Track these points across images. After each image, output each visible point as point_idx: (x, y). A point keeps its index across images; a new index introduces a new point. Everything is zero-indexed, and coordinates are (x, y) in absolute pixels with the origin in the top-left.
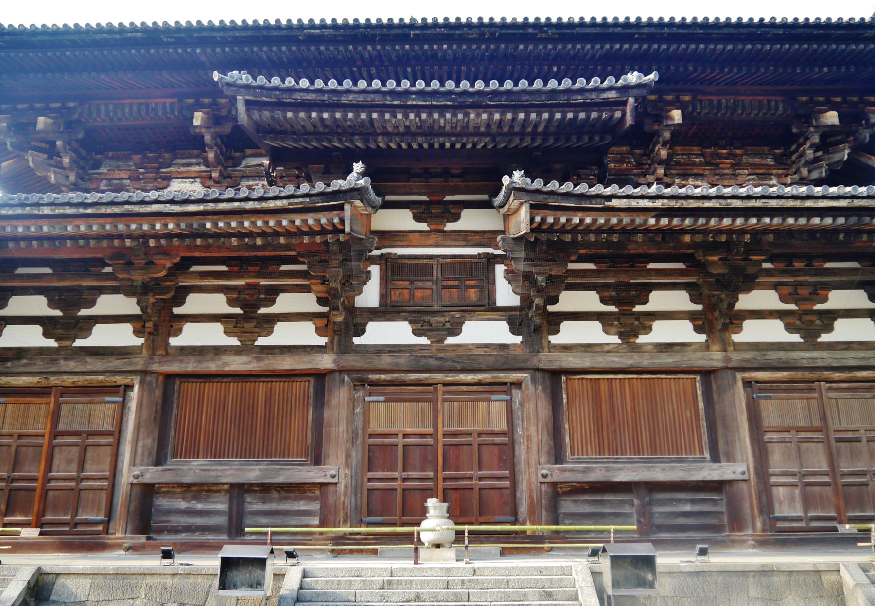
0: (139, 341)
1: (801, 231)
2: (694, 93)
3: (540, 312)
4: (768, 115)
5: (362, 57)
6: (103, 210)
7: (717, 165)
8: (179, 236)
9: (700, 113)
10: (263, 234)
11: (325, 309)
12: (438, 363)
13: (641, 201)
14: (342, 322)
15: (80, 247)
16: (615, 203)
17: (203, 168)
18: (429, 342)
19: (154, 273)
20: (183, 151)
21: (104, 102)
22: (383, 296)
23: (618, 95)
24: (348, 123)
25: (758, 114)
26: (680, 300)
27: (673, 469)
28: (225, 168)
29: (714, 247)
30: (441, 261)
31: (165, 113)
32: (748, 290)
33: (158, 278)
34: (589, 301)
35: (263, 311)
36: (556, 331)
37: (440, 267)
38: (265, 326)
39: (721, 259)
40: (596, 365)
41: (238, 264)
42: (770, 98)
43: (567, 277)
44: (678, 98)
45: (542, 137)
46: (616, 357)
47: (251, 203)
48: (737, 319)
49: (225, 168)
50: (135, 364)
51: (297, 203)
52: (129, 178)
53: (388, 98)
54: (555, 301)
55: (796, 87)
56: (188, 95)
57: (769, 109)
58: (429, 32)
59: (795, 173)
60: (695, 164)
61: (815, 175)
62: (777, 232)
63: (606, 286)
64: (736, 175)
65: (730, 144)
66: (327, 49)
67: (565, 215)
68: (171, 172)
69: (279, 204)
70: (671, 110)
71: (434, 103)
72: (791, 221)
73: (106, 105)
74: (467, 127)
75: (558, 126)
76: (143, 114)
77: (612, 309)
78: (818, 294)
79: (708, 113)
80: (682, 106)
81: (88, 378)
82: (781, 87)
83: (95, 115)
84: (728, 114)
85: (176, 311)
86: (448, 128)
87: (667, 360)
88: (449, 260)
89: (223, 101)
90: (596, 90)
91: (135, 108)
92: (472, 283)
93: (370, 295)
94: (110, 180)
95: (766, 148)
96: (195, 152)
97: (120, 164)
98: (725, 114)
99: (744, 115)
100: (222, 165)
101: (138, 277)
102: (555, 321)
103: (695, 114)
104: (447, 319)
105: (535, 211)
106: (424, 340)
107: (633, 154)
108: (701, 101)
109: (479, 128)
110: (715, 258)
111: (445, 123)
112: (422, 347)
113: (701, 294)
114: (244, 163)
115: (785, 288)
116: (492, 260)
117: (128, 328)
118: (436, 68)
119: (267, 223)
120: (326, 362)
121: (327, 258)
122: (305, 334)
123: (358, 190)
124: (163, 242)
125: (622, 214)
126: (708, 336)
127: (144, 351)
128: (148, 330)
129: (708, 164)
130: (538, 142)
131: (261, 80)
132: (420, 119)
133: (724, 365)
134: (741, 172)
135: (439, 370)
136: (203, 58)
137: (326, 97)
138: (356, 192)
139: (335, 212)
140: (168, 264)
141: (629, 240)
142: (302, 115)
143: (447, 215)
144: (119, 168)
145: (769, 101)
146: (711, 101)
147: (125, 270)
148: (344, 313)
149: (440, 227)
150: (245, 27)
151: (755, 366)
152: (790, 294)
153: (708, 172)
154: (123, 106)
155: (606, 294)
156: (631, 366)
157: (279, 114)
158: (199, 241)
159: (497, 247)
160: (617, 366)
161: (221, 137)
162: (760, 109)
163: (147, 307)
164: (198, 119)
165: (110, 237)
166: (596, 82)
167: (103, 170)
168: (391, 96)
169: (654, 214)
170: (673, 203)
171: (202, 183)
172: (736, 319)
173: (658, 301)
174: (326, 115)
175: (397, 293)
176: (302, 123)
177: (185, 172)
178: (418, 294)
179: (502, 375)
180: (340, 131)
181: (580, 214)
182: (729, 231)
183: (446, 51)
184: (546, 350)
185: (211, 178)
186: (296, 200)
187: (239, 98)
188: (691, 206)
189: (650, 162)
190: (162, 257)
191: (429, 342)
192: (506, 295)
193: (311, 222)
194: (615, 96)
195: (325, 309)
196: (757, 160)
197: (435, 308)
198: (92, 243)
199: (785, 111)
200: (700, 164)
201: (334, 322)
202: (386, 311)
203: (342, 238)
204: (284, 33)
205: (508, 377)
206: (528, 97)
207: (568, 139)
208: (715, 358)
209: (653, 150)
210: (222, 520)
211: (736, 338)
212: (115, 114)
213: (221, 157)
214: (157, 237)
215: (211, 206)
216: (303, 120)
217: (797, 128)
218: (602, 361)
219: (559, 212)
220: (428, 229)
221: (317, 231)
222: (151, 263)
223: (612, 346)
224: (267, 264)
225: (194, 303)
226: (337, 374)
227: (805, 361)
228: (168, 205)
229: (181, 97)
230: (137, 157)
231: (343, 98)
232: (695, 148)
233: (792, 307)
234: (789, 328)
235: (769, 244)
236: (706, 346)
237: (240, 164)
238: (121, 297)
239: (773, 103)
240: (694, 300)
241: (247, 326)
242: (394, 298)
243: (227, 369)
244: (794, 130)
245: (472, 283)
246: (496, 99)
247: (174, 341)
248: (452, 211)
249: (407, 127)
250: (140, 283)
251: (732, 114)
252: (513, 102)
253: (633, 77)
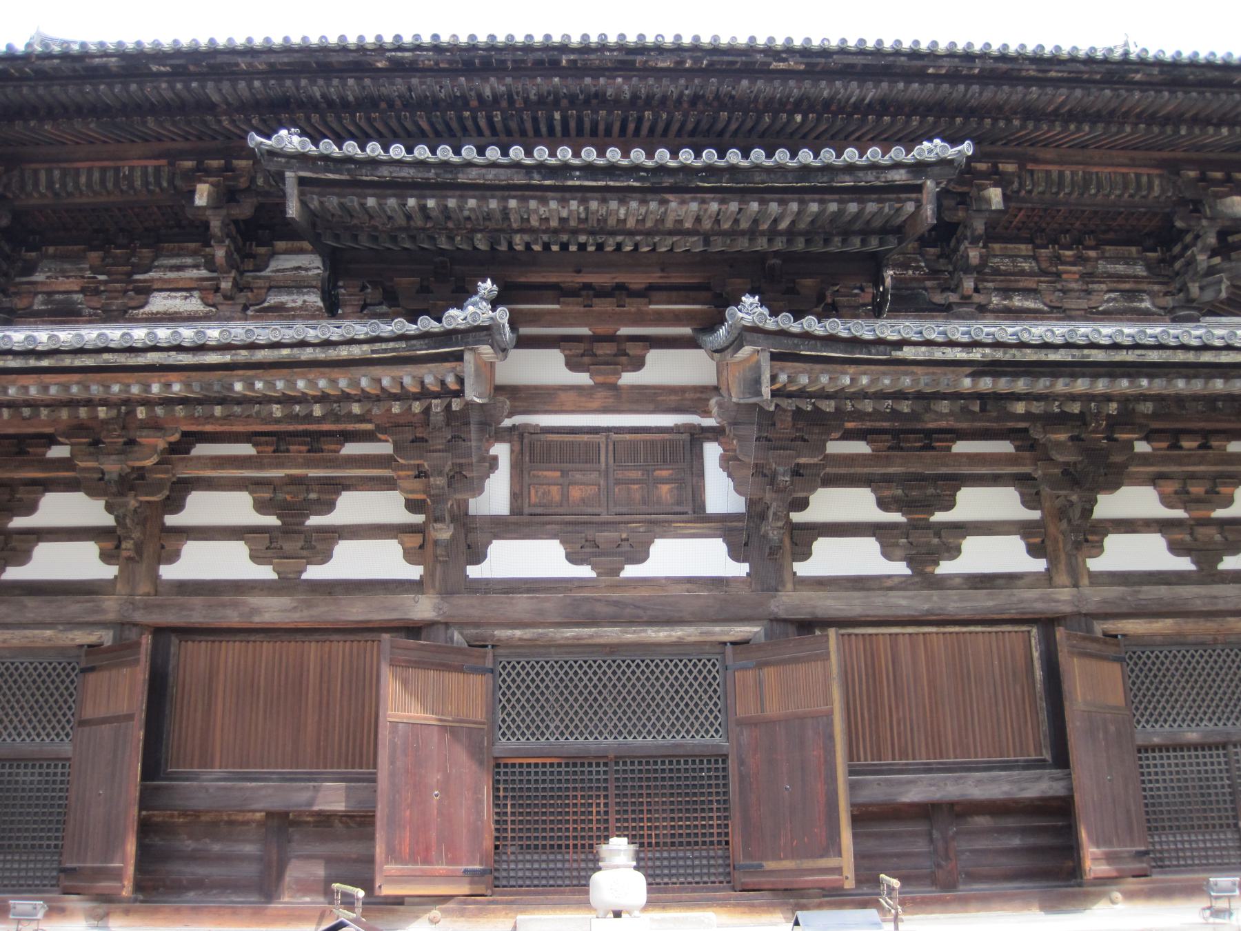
0: (110, 572)
1: (1196, 398)
2: (1022, 160)
3: (780, 524)
4: (1137, 198)
5: (480, 97)
6: (67, 362)
7: (1058, 275)
8: (183, 401)
9: (1030, 192)
10: (323, 398)
11: (419, 519)
12: (610, 610)
13: (949, 350)
14: (446, 539)
15: (24, 419)
16: (908, 353)
17: (204, 273)
18: (594, 575)
19: (138, 459)
20: (172, 245)
21: (46, 166)
22: (516, 496)
23: (909, 176)
24: (466, 213)
25: (1120, 196)
26: (1002, 502)
27: (994, 780)
28: (242, 273)
29: (1062, 419)
30: (614, 436)
31: (146, 183)
32: (1113, 486)
33: (143, 468)
34: (859, 504)
35: (314, 520)
36: (805, 555)
37: (611, 448)
38: (319, 546)
39: (1072, 439)
40: (871, 613)
41: (276, 442)
42: (1139, 170)
43: (824, 467)
44: (995, 166)
45: (785, 239)
46: (904, 597)
47: (309, 350)
48: (1093, 533)
49: (242, 273)
50: (104, 611)
51: (385, 351)
52: (83, 291)
53: (536, 176)
54: (803, 505)
55: (1180, 154)
56: (183, 155)
57: (1139, 187)
58: (593, 57)
59: (1180, 290)
60: (1022, 273)
61: (1208, 295)
62: (1159, 399)
63: (888, 479)
64: (1089, 292)
65: (1078, 242)
66: (422, 83)
67: (828, 372)
68: (152, 280)
69: (356, 351)
70: (985, 188)
71: (612, 183)
72: (1181, 384)
73: (49, 172)
74: (662, 220)
75: (813, 222)
76: (110, 185)
77: (897, 517)
78: (1218, 493)
79: (1043, 193)
80: (1001, 180)
81: (28, 633)
82: (1156, 155)
83: (29, 188)
84: (1075, 195)
85: (171, 520)
86: (631, 224)
87: (984, 602)
88: (628, 437)
89: (242, 163)
90: (874, 167)
91: (96, 176)
92: (665, 473)
93: (495, 496)
94: (50, 294)
95: (1134, 249)
96: (192, 245)
97: (67, 266)
98: (1070, 194)
99: (1099, 197)
100: (238, 269)
101: (112, 467)
102: (802, 539)
103: (1023, 193)
104: (624, 536)
105: (778, 364)
106: (585, 571)
107: (922, 255)
108: (1032, 172)
109: (681, 222)
110: (1063, 437)
111: (626, 214)
112: (580, 583)
113: (1037, 493)
114: (274, 265)
115: (1169, 482)
116: (697, 436)
117: (90, 549)
118: (603, 113)
119: (333, 382)
120: (423, 608)
121: (424, 435)
122: (385, 561)
123: (487, 329)
124: (159, 411)
125: (919, 370)
126: (1050, 562)
127: (119, 586)
128: (125, 554)
129: (1044, 273)
130: (779, 245)
131: (328, 147)
132: (587, 209)
133: (1075, 609)
134: (1096, 286)
135: (614, 621)
136: (215, 98)
137: (432, 174)
138: (484, 332)
139: (448, 365)
140: (161, 444)
141: (928, 409)
142: (392, 202)
143: (624, 359)
144: (64, 273)
145: (1138, 176)
146: (1048, 173)
147: (91, 454)
148: (452, 526)
149: (611, 379)
150: (287, 49)
151: (1124, 610)
152: (1176, 493)
153: (1044, 286)
154: (77, 170)
155: (886, 493)
156: (929, 612)
157: (353, 201)
158: (218, 411)
159: (706, 413)
160: (906, 613)
161: (236, 222)
162: (1125, 188)
163: (125, 516)
164: (202, 195)
165: (73, 404)
166: (874, 154)
167: (39, 277)
168: (539, 173)
169: (968, 370)
170: (999, 355)
171: (202, 299)
172: (1092, 534)
173: (972, 503)
174: (431, 203)
175: (541, 491)
176: (389, 213)
177: (175, 280)
178: (576, 493)
179: (717, 629)
180: (450, 225)
181: (852, 369)
182: (1087, 398)
183: (620, 87)
184: (789, 586)
185: (217, 289)
186: (384, 346)
187: (288, 174)
188: (1027, 359)
189: (951, 268)
190: (151, 432)
191: (594, 575)
192: (721, 494)
193: (407, 381)
194: (904, 177)
195: (419, 519)
196: (1120, 268)
197: (604, 517)
198: (44, 412)
199: (1163, 191)
200: (1031, 274)
201: (436, 543)
202: (521, 523)
203: (456, 405)
204: (351, 57)
205: (728, 633)
206: (764, 176)
207: (827, 241)
208: (1063, 598)
209: (956, 250)
210: (249, 870)
211: (1095, 565)
212: (64, 185)
213: (236, 256)
214: (147, 403)
215: (243, 356)
216: (393, 210)
217: (1182, 219)
218: (880, 604)
219: (818, 367)
220: (591, 382)
221: (414, 394)
222: (131, 442)
223: (896, 580)
224: (317, 442)
225: (201, 508)
226: (442, 628)
227: (1199, 602)
228: (173, 354)
229: (173, 157)
230: (95, 256)
231: (460, 175)
232: (1023, 246)
233: (1179, 513)
234: (1176, 548)
235: (1146, 416)
236: (1047, 578)
237: (267, 266)
238: (79, 497)
239: (1144, 179)
240: (1028, 503)
241: (289, 546)
242: (534, 499)
243: (257, 619)
244: (1179, 224)
245: (665, 473)
246: (713, 179)
247: (168, 572)
248: (631, 352)
249: (562, 220)
250: (115, 477)
251: (1082, 194)
252: (738, 185)
253: (932, 149)
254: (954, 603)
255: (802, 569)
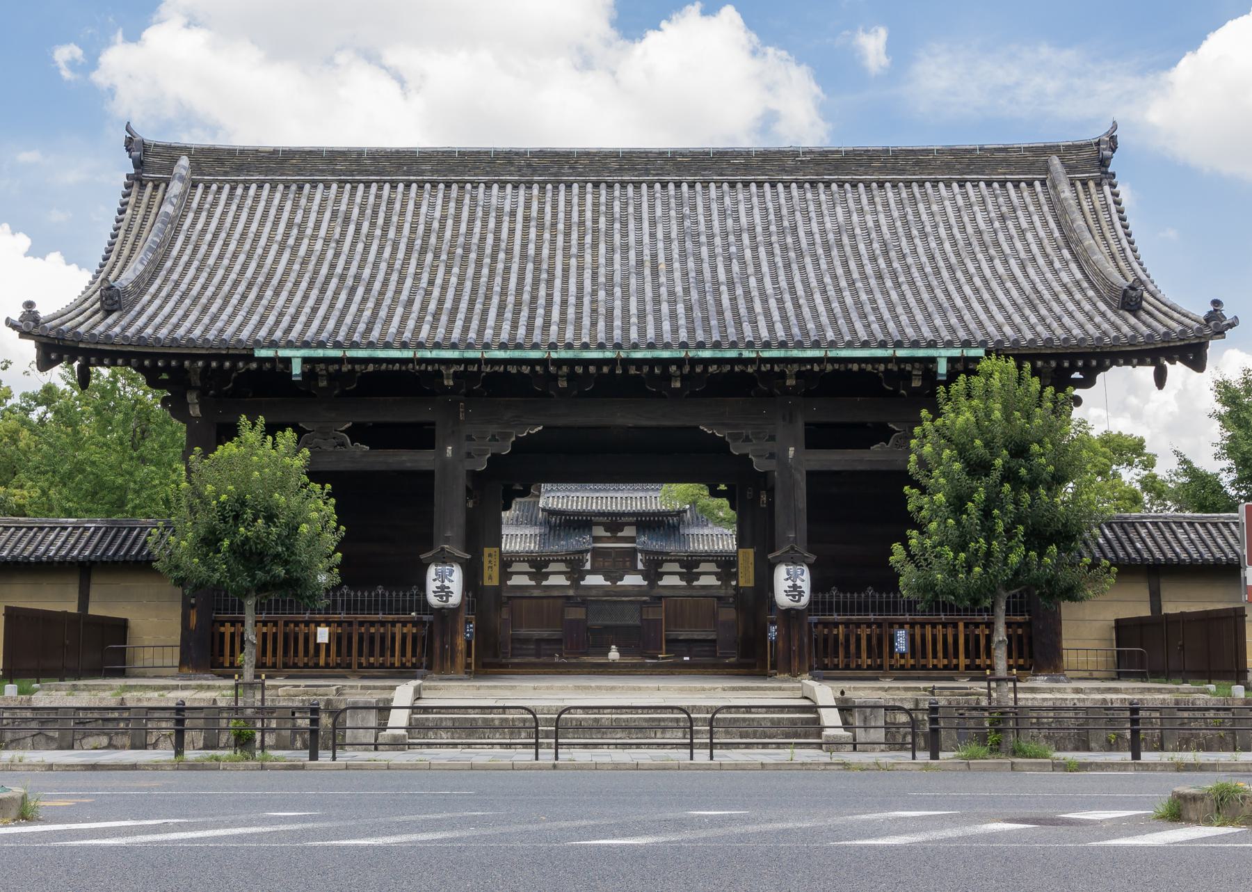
14: (576, 572)
87: (703, 593)
93: (588, 566)
102: (660, 576)
116: (635, 550)
120: (571, 593)
122: (561, 580)
192: (640, 566)
218: (677, 593)
247: (509, 583)
254: (694, 593)
255: (660, 583)
